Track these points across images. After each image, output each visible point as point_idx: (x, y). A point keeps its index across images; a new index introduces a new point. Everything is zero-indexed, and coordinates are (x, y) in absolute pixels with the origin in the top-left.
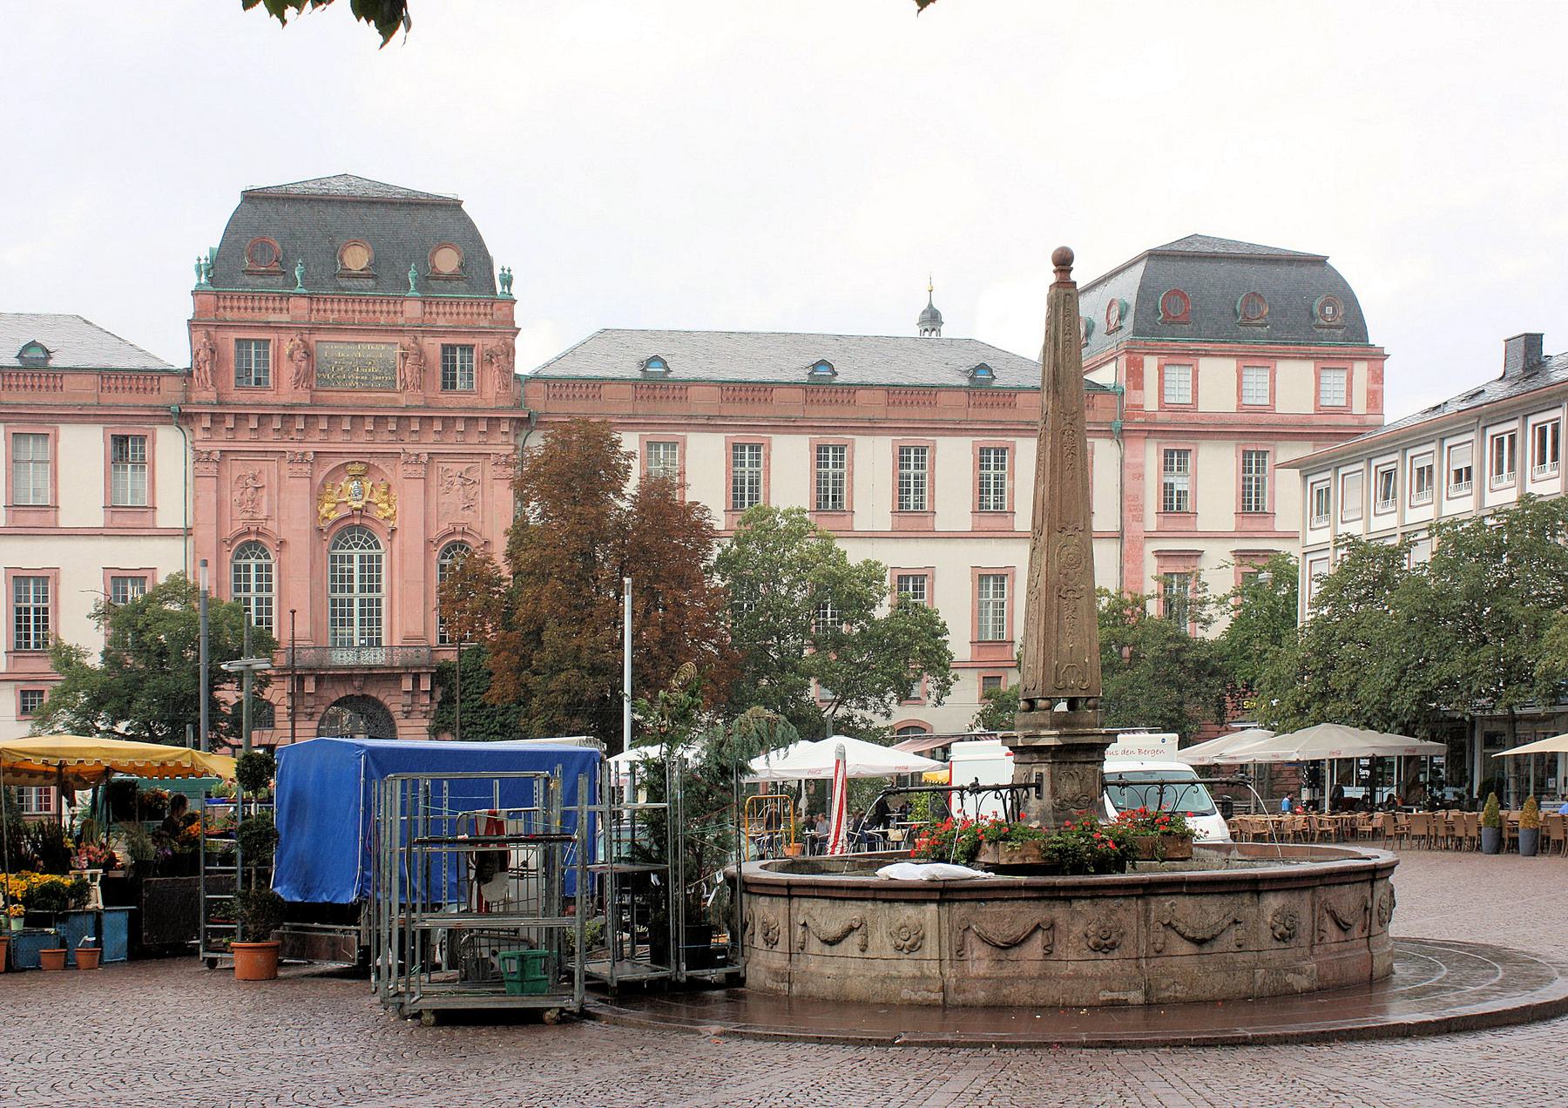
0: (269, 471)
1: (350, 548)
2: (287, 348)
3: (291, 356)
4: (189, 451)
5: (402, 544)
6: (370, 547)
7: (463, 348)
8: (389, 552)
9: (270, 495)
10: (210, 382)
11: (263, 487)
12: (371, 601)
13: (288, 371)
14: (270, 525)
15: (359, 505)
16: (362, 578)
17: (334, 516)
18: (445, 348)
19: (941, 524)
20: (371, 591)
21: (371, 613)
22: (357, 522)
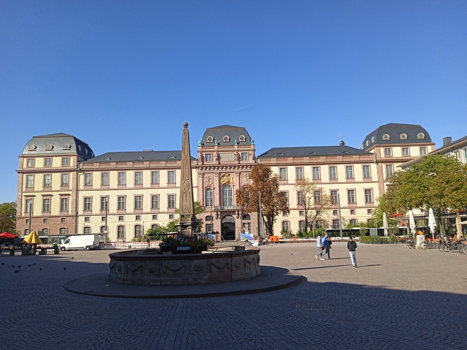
0: (211, 175)
3: (215, 156)
4: (198, 173)
12: (230, 198)
13: (215, 159)
16: (229, 194)
17: (223, 183)
18: (242, 153)
19: (339, 181)
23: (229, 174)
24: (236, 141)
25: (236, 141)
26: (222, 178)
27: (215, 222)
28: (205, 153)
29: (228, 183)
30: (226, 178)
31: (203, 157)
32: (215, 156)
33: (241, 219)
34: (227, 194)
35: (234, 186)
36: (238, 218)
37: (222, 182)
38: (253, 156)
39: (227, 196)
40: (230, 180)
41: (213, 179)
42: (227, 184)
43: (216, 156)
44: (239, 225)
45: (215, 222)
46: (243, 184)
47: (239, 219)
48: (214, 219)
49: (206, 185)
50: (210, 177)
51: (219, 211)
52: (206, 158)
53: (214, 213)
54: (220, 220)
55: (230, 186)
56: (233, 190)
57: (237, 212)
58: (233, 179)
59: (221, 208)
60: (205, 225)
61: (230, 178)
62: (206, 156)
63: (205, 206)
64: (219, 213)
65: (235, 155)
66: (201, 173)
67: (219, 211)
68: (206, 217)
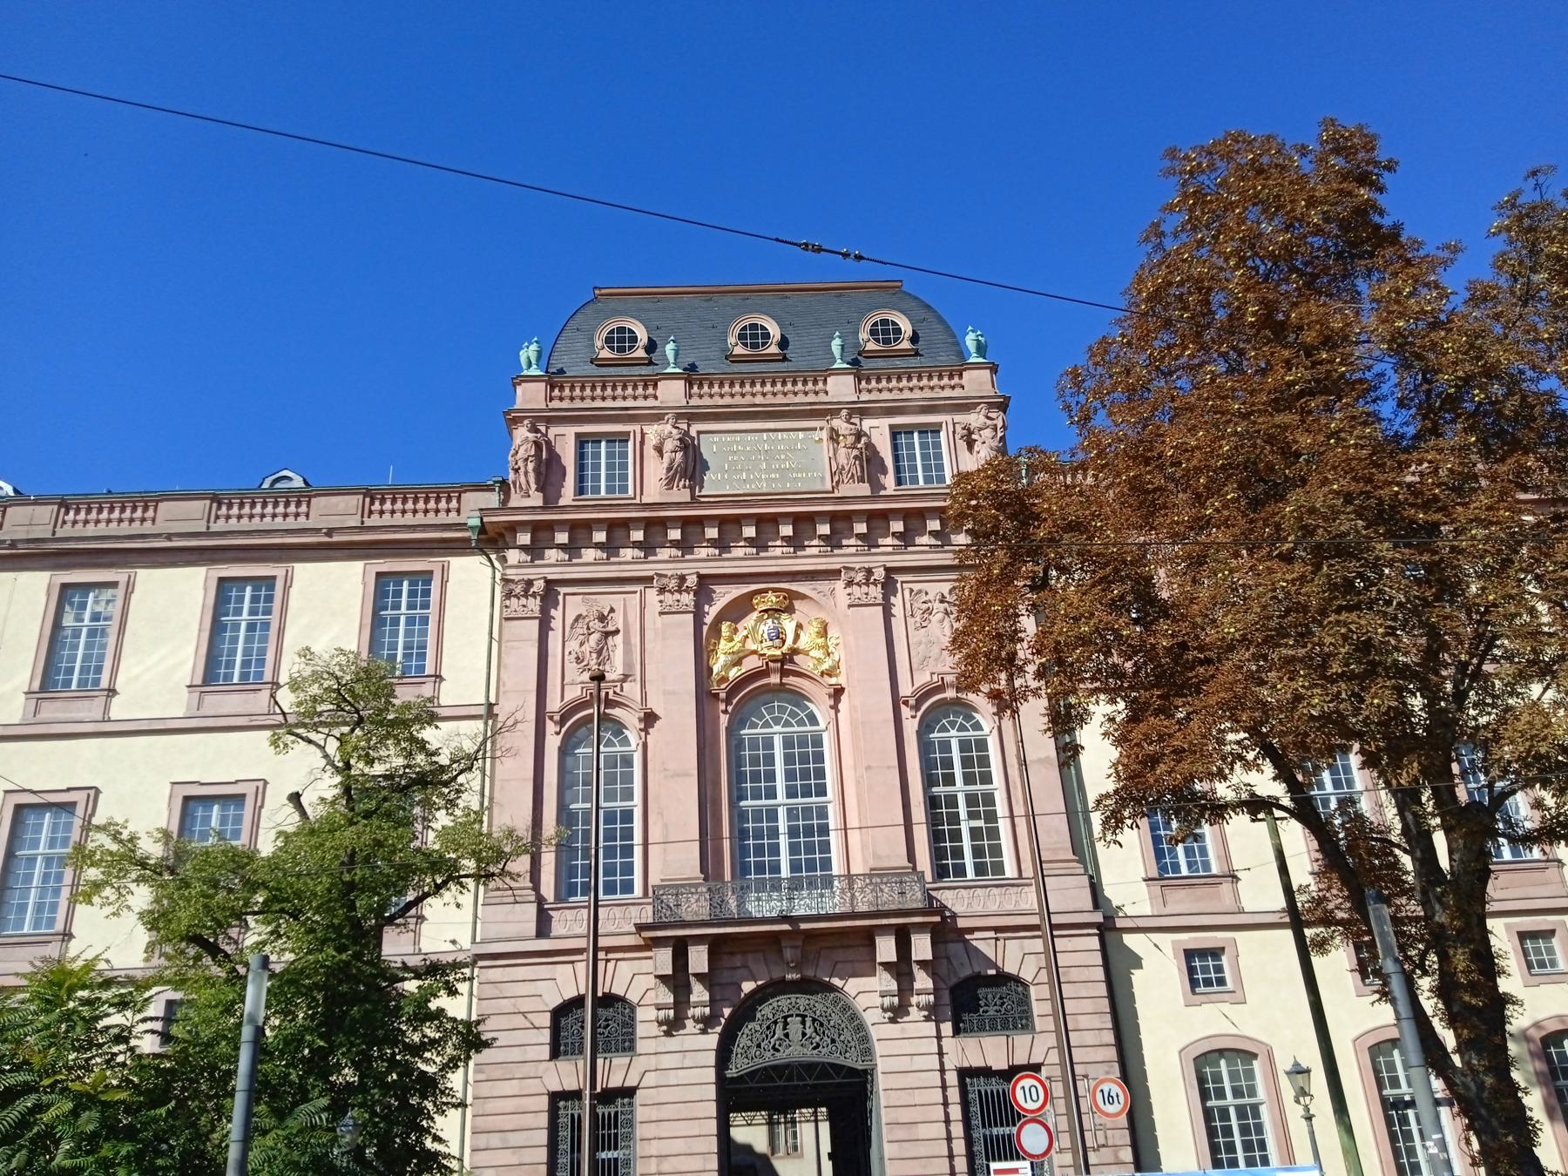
0: (623, 606)
2: (652, 440)
5: (852, 708)
6: (801, 723)
7: (924, 430)
8: (832, 727)
9: (627, 643)
10: (533, 486)
11: (617, 632)
12: (807, 811)
13: (656, 470)
14: (632, 690)
15: (778, 652)
16: (790, 775)
17: (734, 673)
18: (895, 432)
20: (806, 794)
22: (774, 679)
23: (793, 596)
24: (836, 345)
25: (836, 345)
26: (725, 628)
27: (652, 1062)
28: (570, 431)
29: (784, 673)
30: (766, 627)
31: (554, 458)
32: (659, 450)
33: (930, 1028)
34: (771, 776)
35: (838, 693)
36: (897, 1013)
37: (727, 667)
38: (995, 443)
39: (772, 794)
40: (801, 644)
41: (636, 640)
42: (774, 679)
43: (669, 445)
44: (919, 1097)
45: (652, 1062)
46: (923, 678)
47: (917, 1025)
48: (641, 1030)
49: (573, 693)
50: (617, 621)
51: (699, 939)
52: (581, 467)
53: (647, 966)
54: (712, 1040)
55: (799, 698)
57: (886, 949)
58: (824, 632)
59: (717, 903)
60: (544, 1102)
61: (799, 626)
62: (580, 456)
63: (548, 890)
64: (698, 959)
65: (834, 436)
66: (530, 583)
67: (699, 939)
68: (564, 1012)
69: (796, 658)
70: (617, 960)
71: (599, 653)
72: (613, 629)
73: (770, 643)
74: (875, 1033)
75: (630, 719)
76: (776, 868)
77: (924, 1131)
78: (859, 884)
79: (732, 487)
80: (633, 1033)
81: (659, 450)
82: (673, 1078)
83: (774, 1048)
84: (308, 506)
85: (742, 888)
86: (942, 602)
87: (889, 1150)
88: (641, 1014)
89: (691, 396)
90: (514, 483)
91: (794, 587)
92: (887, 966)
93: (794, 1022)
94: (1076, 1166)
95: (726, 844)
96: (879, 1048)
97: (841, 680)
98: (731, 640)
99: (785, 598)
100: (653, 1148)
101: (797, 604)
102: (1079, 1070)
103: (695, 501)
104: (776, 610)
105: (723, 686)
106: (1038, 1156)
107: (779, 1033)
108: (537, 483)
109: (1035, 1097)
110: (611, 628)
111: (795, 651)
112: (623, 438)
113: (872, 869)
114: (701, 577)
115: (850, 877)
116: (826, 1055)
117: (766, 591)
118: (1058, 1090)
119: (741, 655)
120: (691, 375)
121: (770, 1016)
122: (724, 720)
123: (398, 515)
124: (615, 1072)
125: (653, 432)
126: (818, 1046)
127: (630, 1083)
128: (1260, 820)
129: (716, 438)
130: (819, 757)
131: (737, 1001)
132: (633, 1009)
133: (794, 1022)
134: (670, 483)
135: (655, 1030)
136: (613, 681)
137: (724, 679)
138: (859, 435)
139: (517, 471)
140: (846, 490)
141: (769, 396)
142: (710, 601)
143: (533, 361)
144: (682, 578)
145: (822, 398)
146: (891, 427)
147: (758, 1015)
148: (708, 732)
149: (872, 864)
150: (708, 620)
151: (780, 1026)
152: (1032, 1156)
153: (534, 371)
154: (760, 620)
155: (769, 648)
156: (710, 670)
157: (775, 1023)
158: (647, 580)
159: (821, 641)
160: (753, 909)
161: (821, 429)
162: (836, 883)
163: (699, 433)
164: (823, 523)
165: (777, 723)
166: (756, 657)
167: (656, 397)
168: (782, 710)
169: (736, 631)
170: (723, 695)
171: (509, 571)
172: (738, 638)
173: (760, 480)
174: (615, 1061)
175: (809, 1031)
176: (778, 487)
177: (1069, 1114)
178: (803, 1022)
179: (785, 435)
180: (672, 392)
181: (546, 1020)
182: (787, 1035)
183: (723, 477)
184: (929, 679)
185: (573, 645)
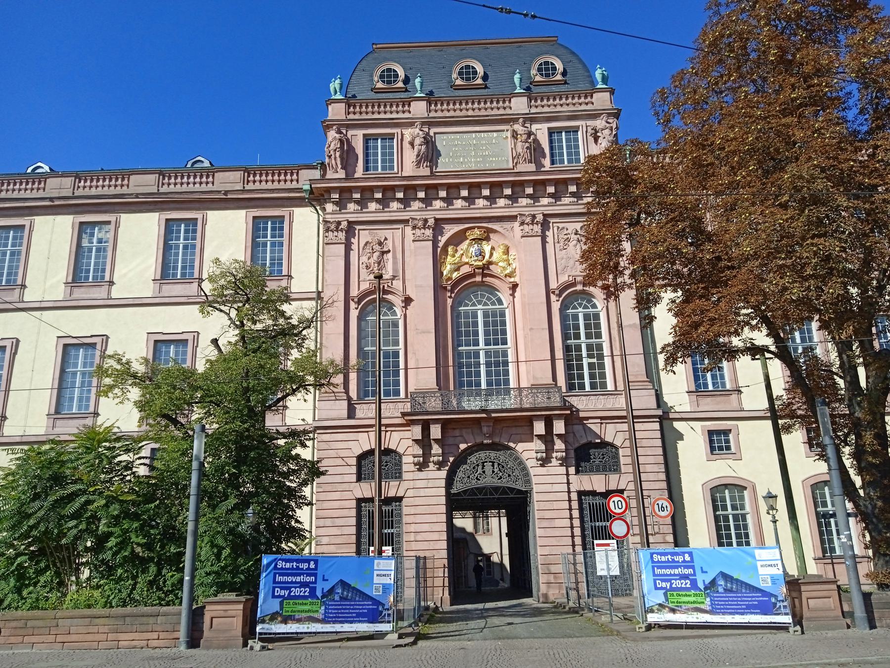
0: (392, 236)
1: (474, 305)
2: (407, 138)
5: (523, 296)
6: (493, 304)
9: (395, 258)
10: (340, 166)
11: (389, 251)
12: (496, 353)
13: (410, 156)
14: (397, 284)
15: (481, 263)
16: (487, 333)
17: (455, 275)
18: (551, 132)
20: (496, 344)
21: (498, 365)
22: (478, 279)
23: (489, 231)
24: (517, 78)
25: (517, 78)
26: (450, 249)
27: (411, 484)
28: (360, 133)
29: (484, 275)
30: (473, 250)
31: (351, 149)
32: (412, 144)
33: (563, 470)
34: (476, 334)
35: (514, 287)
36: (545, 462)
38: (611, 138)
39: (476, 343)
40: (494, 259)
41: (399, 256)
42: (478, 279)
43: (418, 141)
44: (556, 505)
45: (411, 484)
46: (564, 279)
47: (556, 469)
48: (405, 468)
49: (365, 286)
50: (389, 245)
51: (436, 421)
52: (366, 155)
53: (408, 434)
54: (443, 474)
55: (492, 289)
56: (508, 313)
57: (539, 428)
58: (507, 252)
59: (446, 402)
60: (353, 504)
61: (493, 248)
62: (366, 148)
63: (353, 394)
64: (436, 432)
65: (515, 135)
66: (339, 223)
67: (436, 421)
68: (362, 458)
69: (491, 267)
70: (392, 431)
71: (379, 263)
72: (387, 250)
73: (476, 258)
74: (532, 472)
75: (397, 301)
76: (479, 384)
77: (558, 523)
78: (525, 393)
79: (455, 167)
80: (401, 469)
81: (412, 144)
82: (422, 492)
83: (477, 478)
84: (213, 178)
85: (460, 394)
86: (576, 234)
87: (539, 532)
88: (405, 459)
89: (430, 111)
90: (329, 164)
91: (490, 225)
92: (539, 437)
93: (488, 466)
94: (642, 543)
95: (451, 369)
96: (534, 480)
97: (516, 279)
98: (454, 256)
99: (485, 232)
100: (412, 528)
101: (491, 235)
102: (645, 493)
103: (433, 175)
104: (480, 239)
105: (449, 283)
106: (621, 537)
107: (480, 471)
108: (342, 164)
109: (620, 507)
110: (385, 249)
111: (490, 263)
112: (391, 137)
113: (532, 385)
114: (436, 220)
115: (520, 389)
116: (505, 483)
117: (474, 228)
118: (633, 503)
119: (459, 265)
120: (430, 98)
121: (475, 462)
122: (450, 301)
123: (264, 183)
124: (392, 489)
125: (408, 133)
126: (501, 478)
127: (400, 494)
128: (757, 359)
129: (445, 136)
130: (504, 323)
131: (457, 454)
132: (400, 456)
133: (488, 466)
134: (418, 164)
135: (412, 468)
136: (387, 280)
137: (449, 279)
138: (530, 134)
139: (330, 157)
140: (521, 168)
141: (477, 110)
142: (442, 234)
143: (338, 90)
144: (426, 221)
145: (508, 111)
146: (549, 129)
147: (469, 461)
148: (441, 309)
149: (532, 382)
150: (441, 244)
151: (480, 467)
152: (618, 537)
153: (339, 96)
154: (470, 245)
155: (475, 261)
156: (442, 273)
157: (478, 465)
158: (405, 222)
159: (505, 257)
160: (465, 405)
161: (507, 130)
162: (512, 392)
163: (435, 134)
164: (551, 185)
165: (480, 304)
166: (468, 266)
167: (410, 112)
168: (482, 296)
169: (456, 251)
170: (449, 288)
171: (327, 216)
172: (457, 255)
173: (471, 162)
174: (391, 483)
175: (496, 470)
176: (481, 166)
177: (639, 516)
178: (493, 466)
179: (486, 135)
180: (419, 109)
181: (354, 461)
182: (484, 472)
183: (449, 160)
184: (567, 279)
185: (364, 259)
